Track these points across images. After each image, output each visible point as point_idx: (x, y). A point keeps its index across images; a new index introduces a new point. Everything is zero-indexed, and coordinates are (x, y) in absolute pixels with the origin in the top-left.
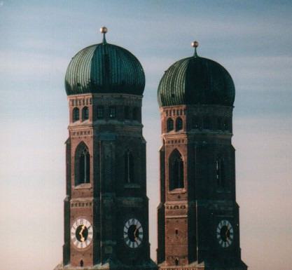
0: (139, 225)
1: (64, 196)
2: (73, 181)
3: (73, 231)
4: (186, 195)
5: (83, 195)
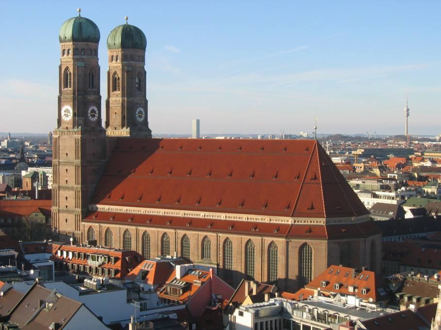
0: (96, 109)
1: (58, 94)
2: (62, 87)
3: (63, 113)
4: (121, 95)
5: (68, 94)
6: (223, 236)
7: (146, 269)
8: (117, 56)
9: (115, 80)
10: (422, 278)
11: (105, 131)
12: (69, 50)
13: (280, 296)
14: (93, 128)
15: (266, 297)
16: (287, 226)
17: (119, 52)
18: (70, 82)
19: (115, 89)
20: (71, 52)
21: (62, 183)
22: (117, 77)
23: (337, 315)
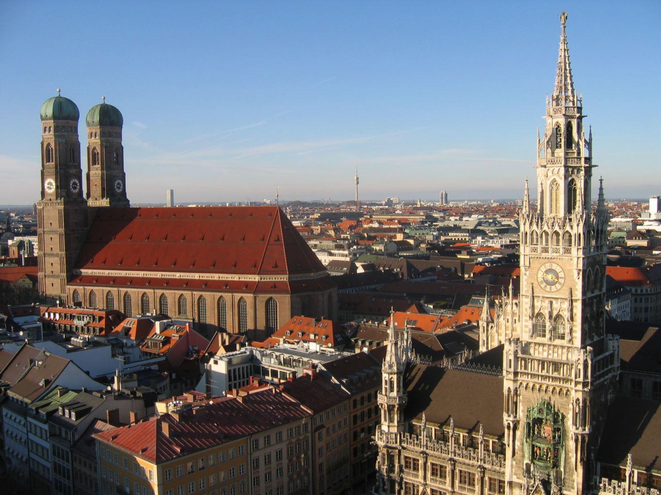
0: (77, 181)
1: (41, 168)
2: (45, 161)
3: (46, 185)
4: (100, 168)
5: (50, 168)
6: (197, 294)
7: (128, 326)
8: (96, 133)
9: (94, 155)
10: (373, 325)
11: (86, 202)
12: (50, 127)
13: (250, 345)
14: (75, 199)
15: (238, 346)
16: (255, 282)
17: (97, 130)
18: (52, 157)
19: (94, 163)
20: (52, 129)
21: (48, 251)
22: (96, 152)
23: (301, 360)
